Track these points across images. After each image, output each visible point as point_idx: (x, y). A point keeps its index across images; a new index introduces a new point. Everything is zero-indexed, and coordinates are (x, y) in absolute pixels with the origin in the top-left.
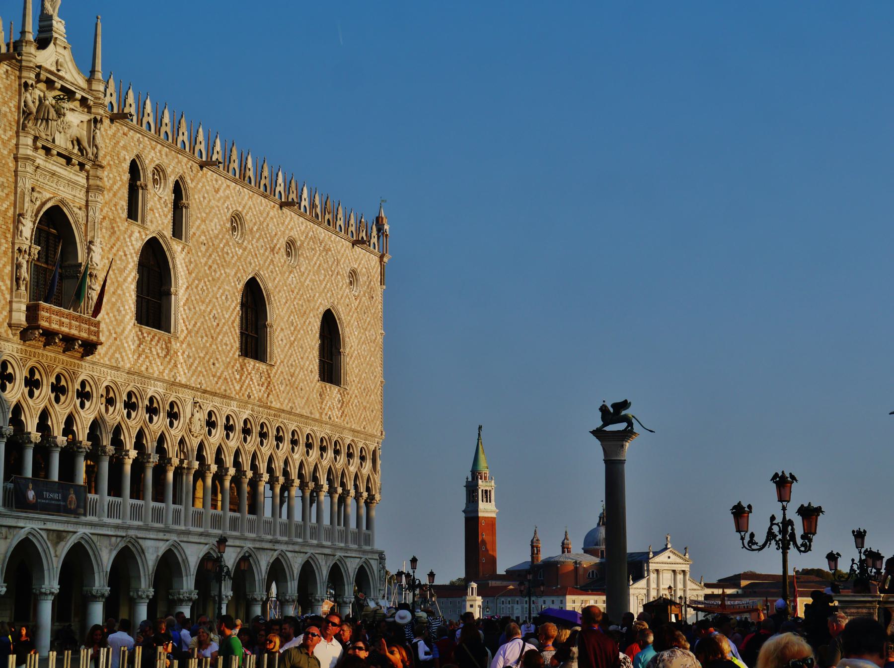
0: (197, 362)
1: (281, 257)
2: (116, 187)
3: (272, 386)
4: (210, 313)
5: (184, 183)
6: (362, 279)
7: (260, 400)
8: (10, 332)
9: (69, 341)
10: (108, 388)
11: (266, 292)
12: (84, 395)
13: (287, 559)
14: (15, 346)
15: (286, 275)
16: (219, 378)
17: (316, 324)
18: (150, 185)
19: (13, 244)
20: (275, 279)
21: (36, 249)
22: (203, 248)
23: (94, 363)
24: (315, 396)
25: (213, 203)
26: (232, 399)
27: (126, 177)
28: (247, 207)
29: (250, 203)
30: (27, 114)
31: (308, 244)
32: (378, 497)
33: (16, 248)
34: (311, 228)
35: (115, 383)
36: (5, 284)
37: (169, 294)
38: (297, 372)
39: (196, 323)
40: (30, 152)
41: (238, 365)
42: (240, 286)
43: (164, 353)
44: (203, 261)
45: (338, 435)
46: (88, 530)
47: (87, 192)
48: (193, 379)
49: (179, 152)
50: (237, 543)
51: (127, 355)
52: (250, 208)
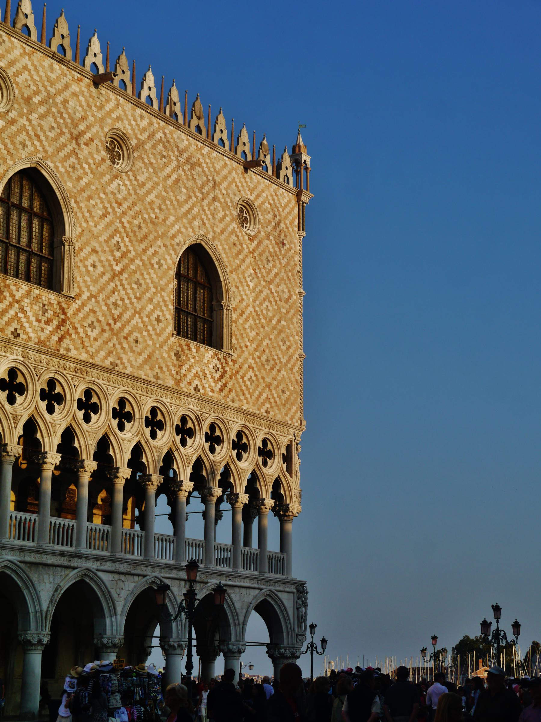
3: (68, 326)
7: (39, 342)
11: (62, 193)
13: (101, 583)
15: (107, 177)
17: (171, 260)
20: (79, 178)
24: (165, 355)
28: (19, 66)
29: (25, 60)
31: (154, 147)
32: (295, 507)
34: (159, 128)
38: (126, 316)
45: (213, 415)
52: (25, 68)
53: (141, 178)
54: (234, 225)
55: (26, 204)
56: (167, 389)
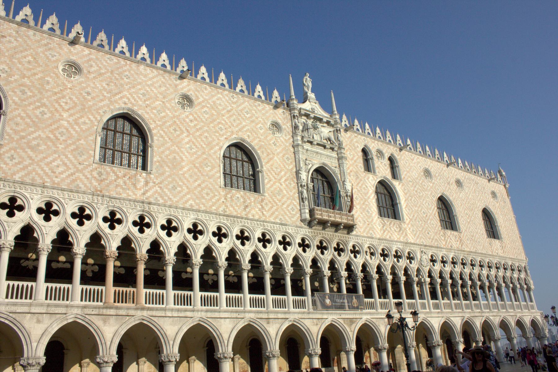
0: (418, 233)
1: (454, 186)
2: (355, 158)
4: (421, 210)
5: (394, 157)
6: (498, 195)
8: (302, 224)
9: (336, 226)
10: (369, 247)
12: (355, 252)
14: (307, 230)
16: (433, 239)
17: (480, 214)
18: (375, 158)
19: (297, 183)
21: (311, 185)
22: (411, 184)
23: (357, 236)
25: (411, 164)
26: (442, 248)
27: (361, 154)
29: (432, 164)
30: (296, 127)
32: (532, 287)
33: (299, 185)
35: (373, 245)
36: (296, 202)
37: (397, 204)
39: (414, 216)
40: (300, 142)
41: (442, 233)
42: (435, 199)
43: (398, 229)
44: (412, 189)
46: (369, 317)
47: (338, 160)
48: (418, 240)
49: (388, 144)
50: (460, 315)
51: (377, 231)
53: (467, 191)
54: (492, 199)
55: (441, 207)
56: (490, 255)
